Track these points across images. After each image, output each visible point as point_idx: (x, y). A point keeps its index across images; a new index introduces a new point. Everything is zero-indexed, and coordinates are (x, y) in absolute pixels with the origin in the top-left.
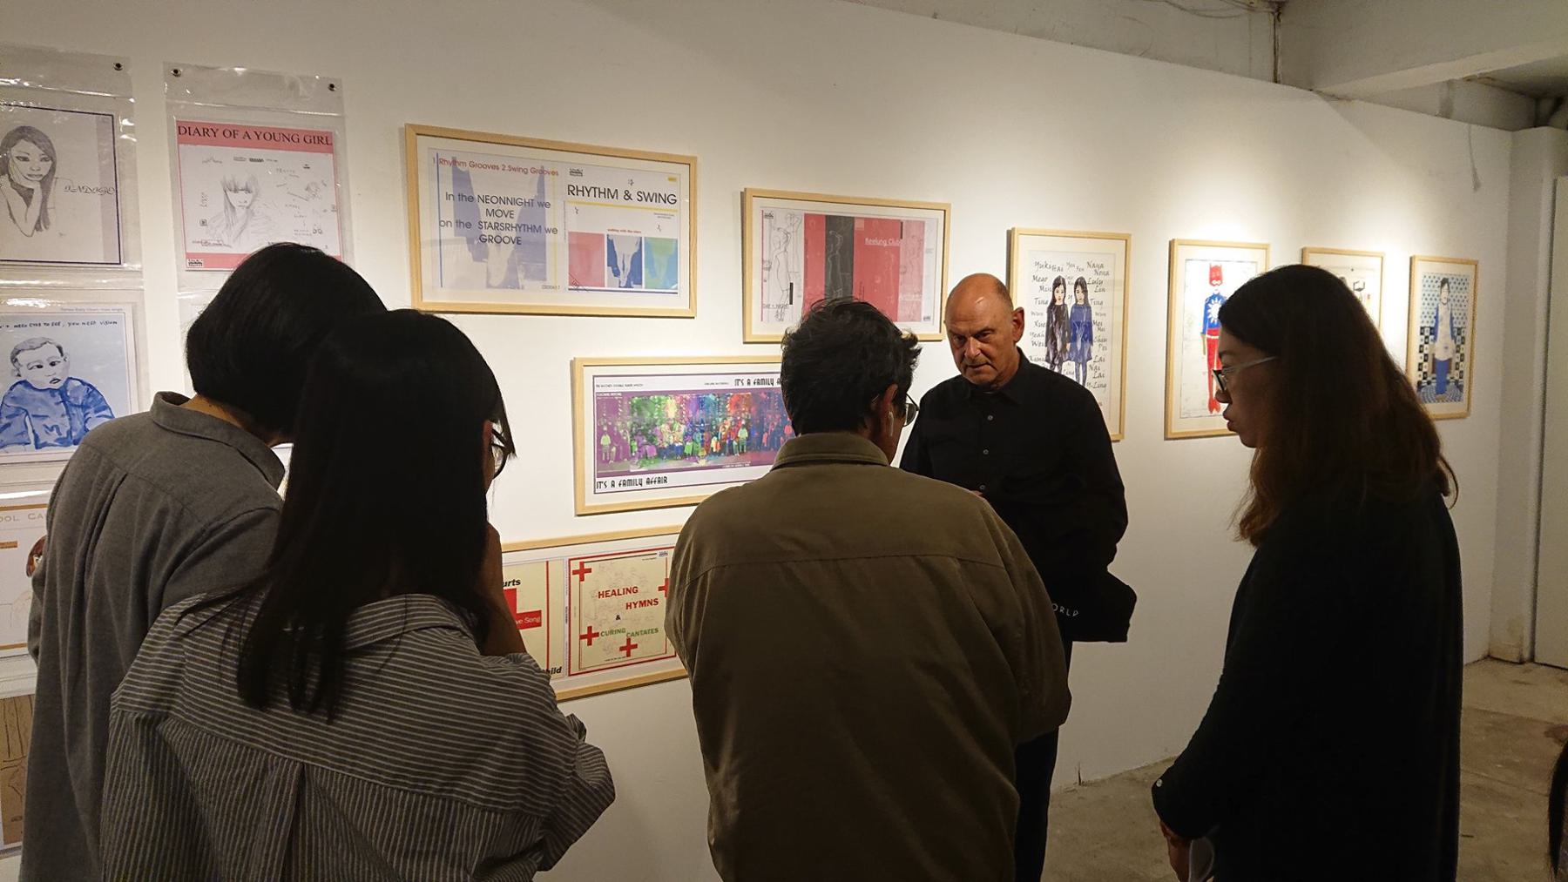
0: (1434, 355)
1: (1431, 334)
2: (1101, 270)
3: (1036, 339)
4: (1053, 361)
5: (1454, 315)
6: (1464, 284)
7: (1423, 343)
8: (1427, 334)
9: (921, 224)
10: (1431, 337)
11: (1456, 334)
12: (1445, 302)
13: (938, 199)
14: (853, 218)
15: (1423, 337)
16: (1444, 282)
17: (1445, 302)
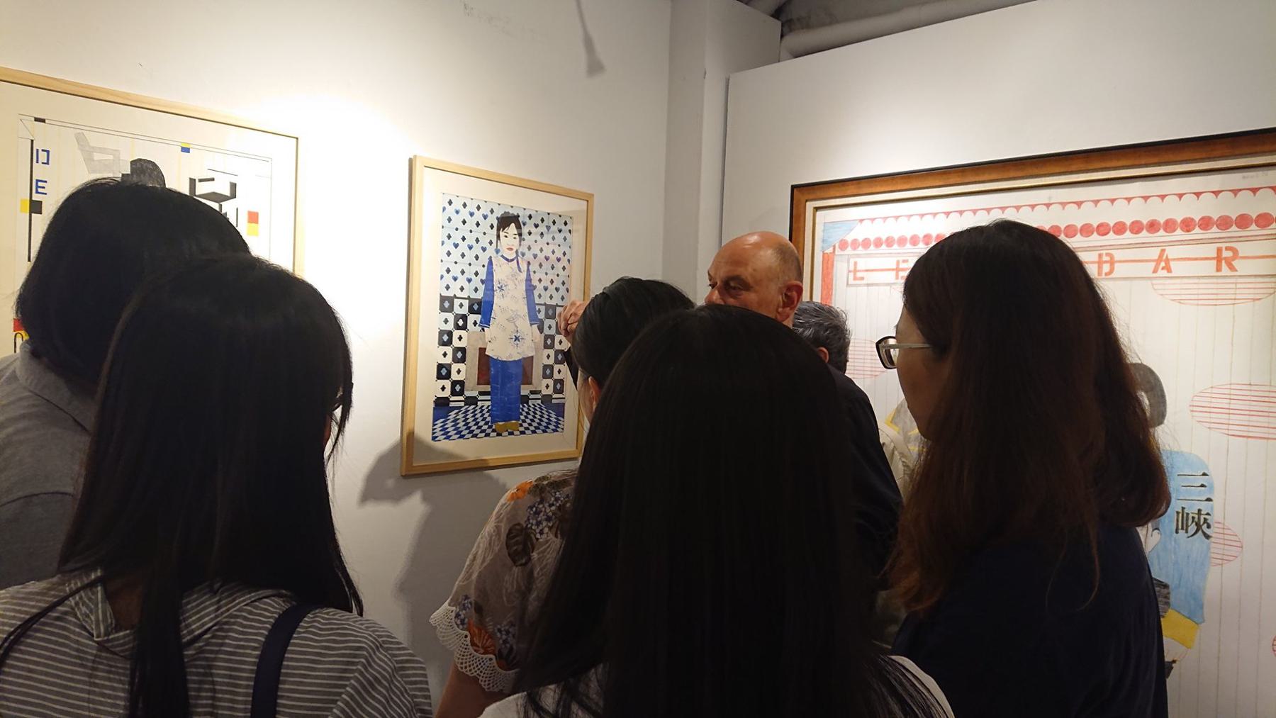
0: (482, 350)
1: (471, 311)
5: (535, 282)
8: (465, 311)
11: (541, 316)
12: (511, 255)
16: (506, 221)
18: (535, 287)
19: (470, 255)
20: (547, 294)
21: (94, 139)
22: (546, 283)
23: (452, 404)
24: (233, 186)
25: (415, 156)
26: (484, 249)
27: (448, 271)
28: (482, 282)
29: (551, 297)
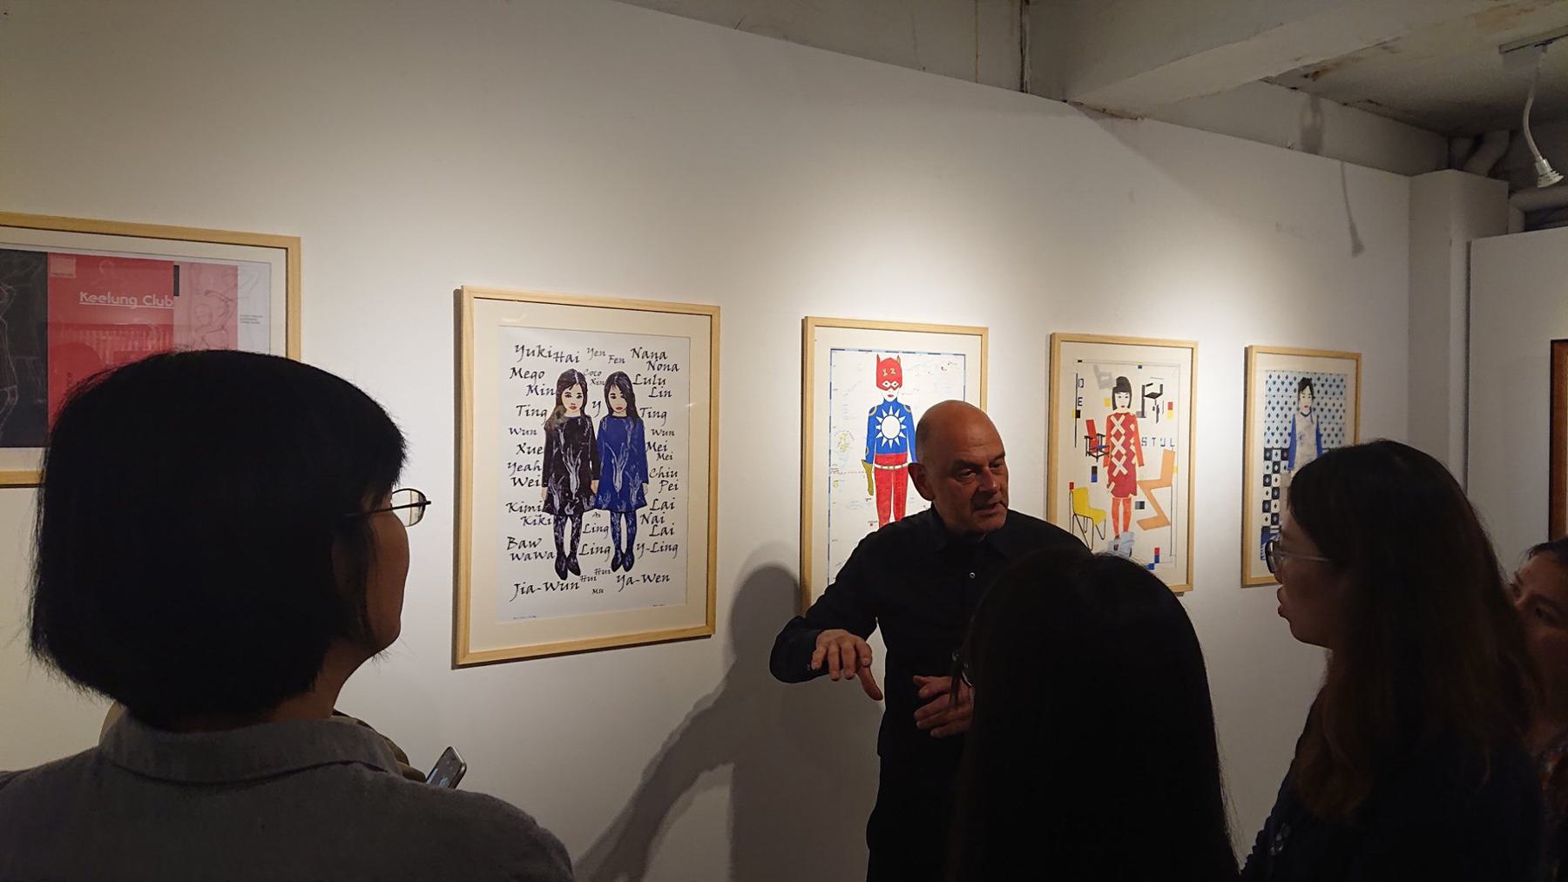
1: (1283, 458)
2: (662, 361)
3: (521, 475)
4: (562, 511)
5: (1321, 432)
6: (1338, 386)
7: (1269, 472)
8: (1278, 458)
9: (230, 273)
10: (1284, 463)
12: (1306, 411)
13: (284, 231)
14: (46, 253)
15: (1270, 463)
16: (1305, 383)
17: (1306, 411)
18: (1321, 435)
19: (1282, 414)
20: (1329, 440)
21: (1102, 369)
22: (1328, 431)
23: (1272, 532)
24: (1161, 386)
25: (1251, 347)
26: (1290, 409)
27: (1269, 429)
28: (1289, 434)
29: (1332, 442)
